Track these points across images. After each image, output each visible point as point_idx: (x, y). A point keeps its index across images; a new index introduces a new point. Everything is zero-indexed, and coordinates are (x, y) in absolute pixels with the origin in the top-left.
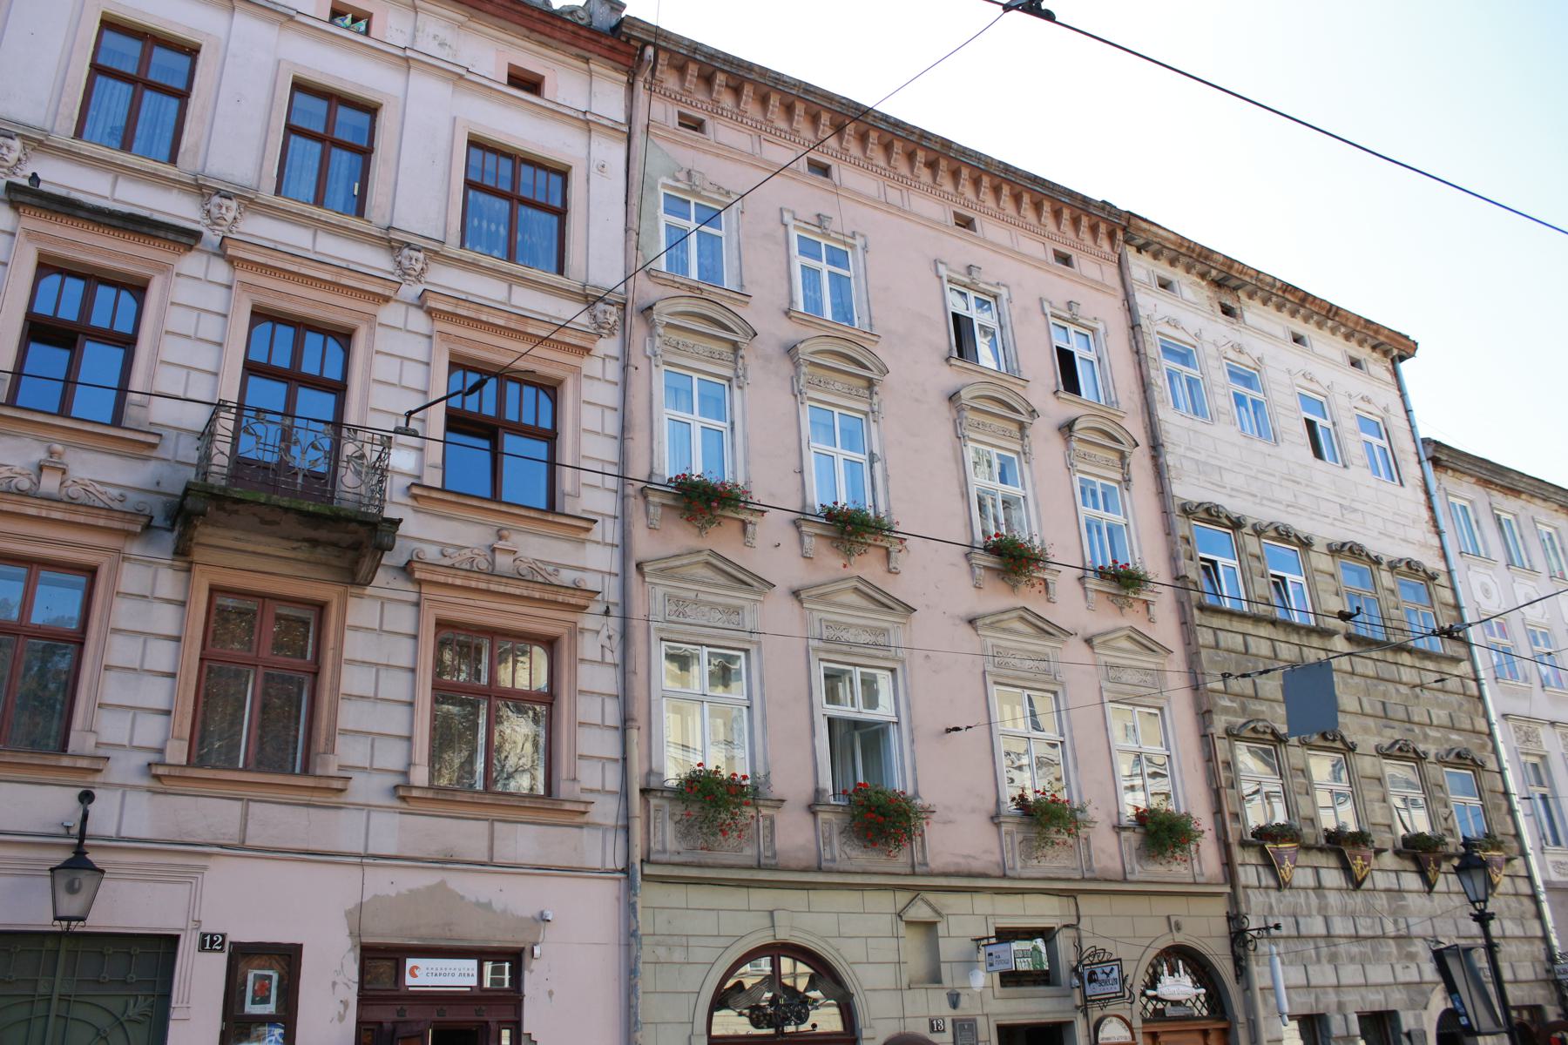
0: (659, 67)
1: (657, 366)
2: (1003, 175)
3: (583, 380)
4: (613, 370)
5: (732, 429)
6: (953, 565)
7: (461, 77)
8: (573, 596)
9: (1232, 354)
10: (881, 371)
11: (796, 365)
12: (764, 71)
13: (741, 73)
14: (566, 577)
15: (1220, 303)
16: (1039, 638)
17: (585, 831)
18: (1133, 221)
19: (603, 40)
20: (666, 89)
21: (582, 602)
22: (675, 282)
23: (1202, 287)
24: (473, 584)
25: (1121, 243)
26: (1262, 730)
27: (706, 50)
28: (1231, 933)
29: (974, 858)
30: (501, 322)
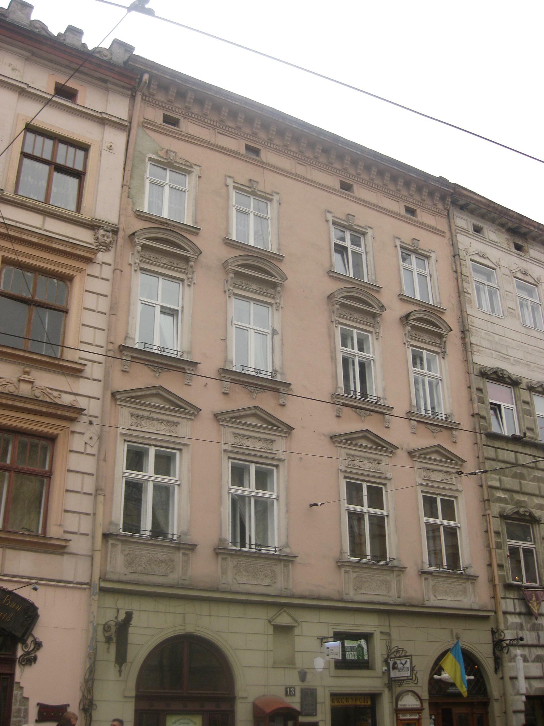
0: (152, 86)
1: (136, 271)
3: (86, 277)
4: (107, 272)
5: (182, 311)
8: (68, 411)
9: (519, 275)
10: (282, 278)
11: (227, 273)
14: (67, 400)
15: (514, 243)
16: (376, 450)
20: (156, 100)
21: (73, 415)
22: (152, 219)
23: (502, 233)
25: (450, 203)
26: (523, 513)
28: (493, 641)
30: (35, 240)
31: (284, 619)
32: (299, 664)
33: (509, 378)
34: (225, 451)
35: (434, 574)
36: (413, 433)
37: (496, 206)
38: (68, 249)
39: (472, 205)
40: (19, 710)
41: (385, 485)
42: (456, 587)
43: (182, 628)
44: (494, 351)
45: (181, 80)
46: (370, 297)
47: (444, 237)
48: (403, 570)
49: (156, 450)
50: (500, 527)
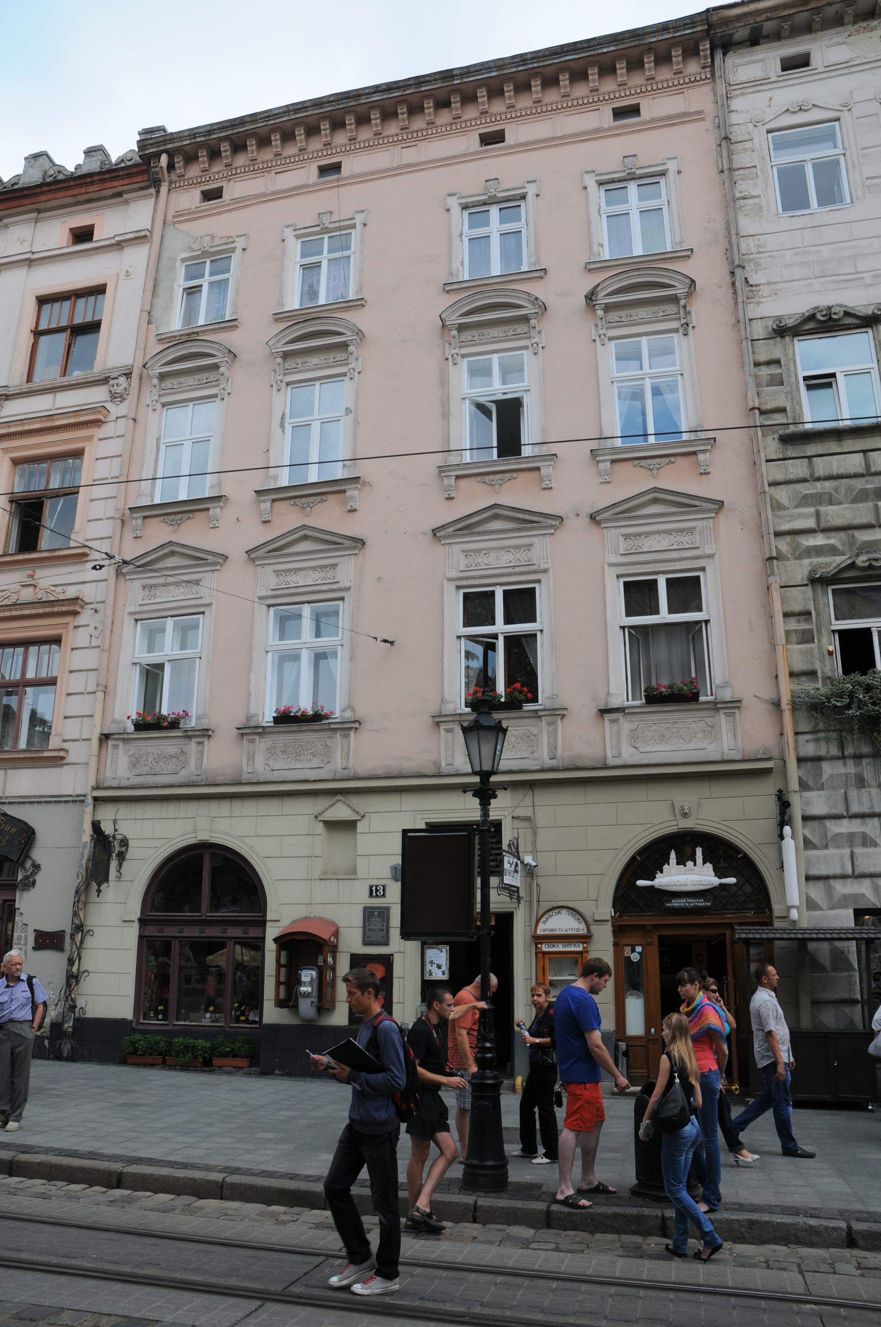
10: (353, 331)
12: (254, 118)
13: (235, 131)
14: (71, 592)
16: (519, 530)
21: (70, 608)
22: (175, 336)
31: (340, 811)
33: (847, 314)
34: (261, 598)
35: (626, 711)
36: (602, 483)
38: (72, 421)
40: (20, 937)
42: (689, 726)
43: (194, 835)
46: (512, 294)
50: (812, 603)
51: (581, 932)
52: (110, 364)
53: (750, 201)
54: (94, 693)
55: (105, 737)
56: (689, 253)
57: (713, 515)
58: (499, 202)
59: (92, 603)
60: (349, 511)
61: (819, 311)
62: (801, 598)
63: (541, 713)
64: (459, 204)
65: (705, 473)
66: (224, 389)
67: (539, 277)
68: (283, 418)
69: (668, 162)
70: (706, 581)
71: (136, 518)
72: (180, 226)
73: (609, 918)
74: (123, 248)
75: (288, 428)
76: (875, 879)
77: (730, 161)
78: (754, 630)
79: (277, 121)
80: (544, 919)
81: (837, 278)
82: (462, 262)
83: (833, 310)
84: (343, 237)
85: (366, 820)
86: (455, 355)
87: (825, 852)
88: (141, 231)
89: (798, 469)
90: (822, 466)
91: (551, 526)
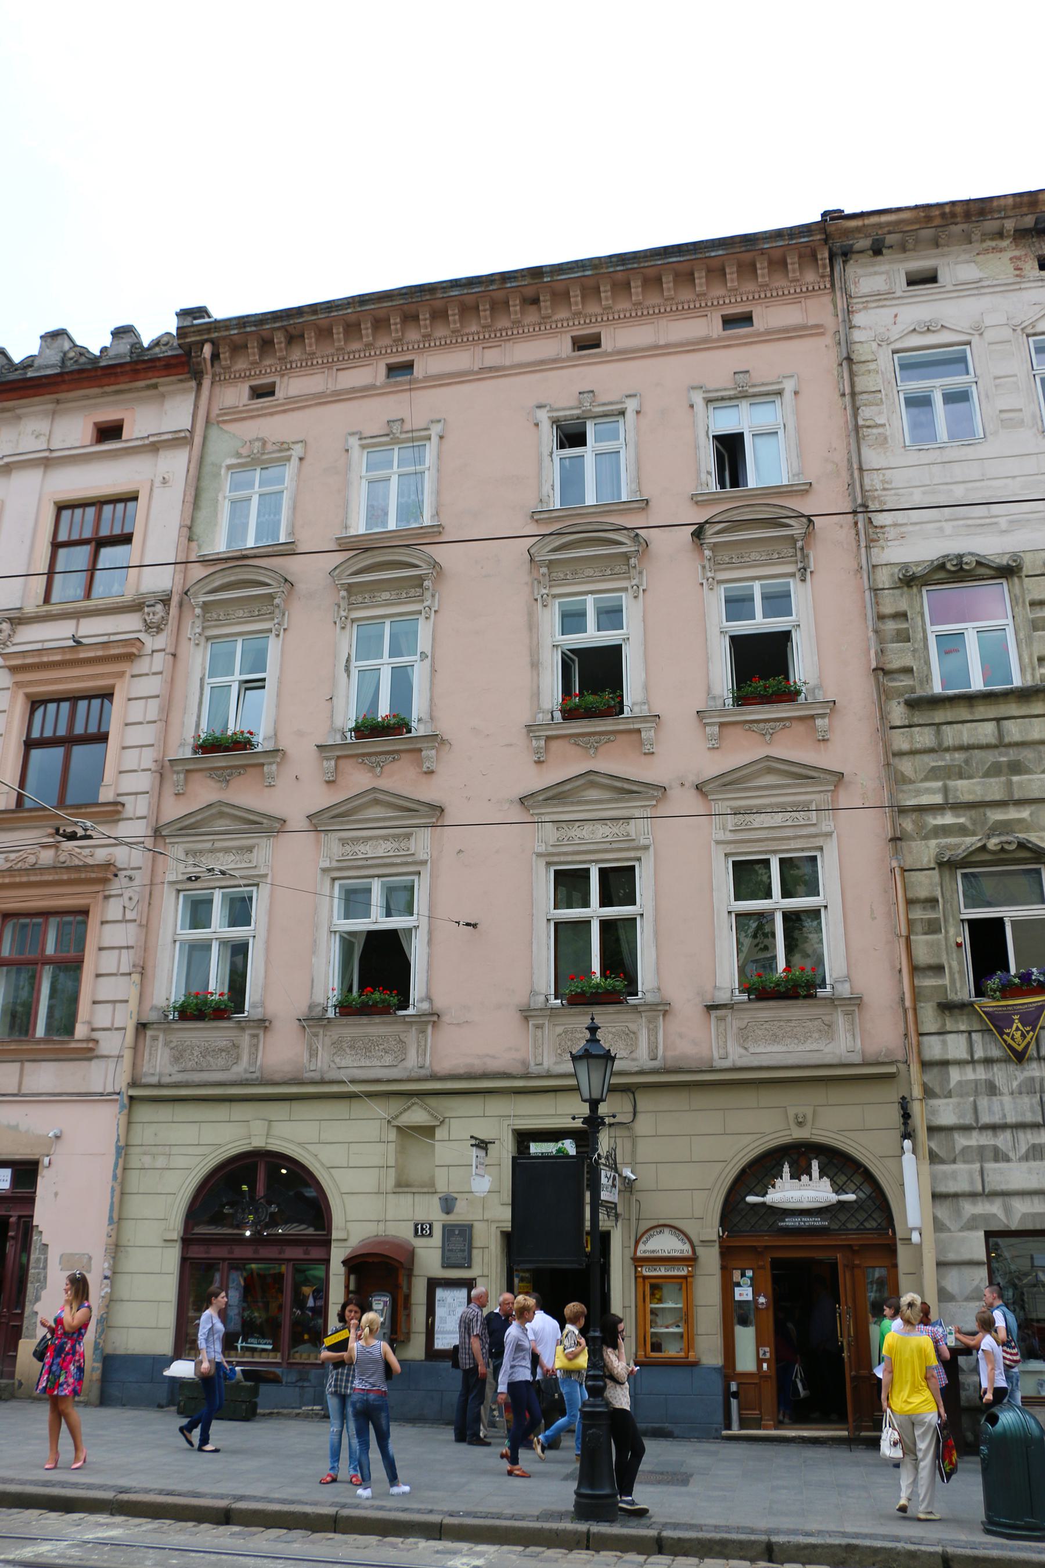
2: (619, 268)
4: (159, 662)
6: (511, 745)
7: (46, 458)
10: (429, 564)
12: (314, 309)
13: (292, 322)
16: (616, 800)
17: (94, 1063)
18: (831, 229)
19: (158, 364)
20: (235, 372)
24: (18, 880)
27: (253, 319)
29: (494, 1057)
30: (57, 658)
31: (417, 1116)
32: (441, 1186)
33: (979, 564)
35: (735, 1007)
36: (709, 749)
37: (947, 209)
38: (100, 653)
39: (888, 237)
41: (639, 859)
43: (247, 1141)
44: (946, 520)
45: (255, 326)
47: (822, 334)
48: (660, 1008)
49: (224, 895)
50: (939, 889)
51: (685, 1254)
52: (144, 589)
53: (875, 431)
54: (130, 974)
55: (142, 1027)
56: (807, 487)
57: (832, 788)
58: (595, 417)
59: (125, 869)
60: (426, 773)
61: (949, 560)
62: (926, 884)
63: (641, 1009)
64: (549, 417)
65: (823, 740)
66: (279, 624)
67: (639, 508)
68: (348, 660)
69: (785, 381)
70: (823, 861)
71: (178, 773)
72: (226, 427)
73: (715, 1237)
74: (157, 450)
75: (354, 673)
76: (1007, 1199)
77: (852, 385)
78: (875, 918)
79: (341, 313)
80: (644, 1239)
81: (970, 522)
82: (553, 486)
83: (965, 560)
84: (416, 449)
85: (445, 1127)
86: (545, 596)
87: (954, 1167)
88: (180, 431)
89: (924, 738)
90: (951, 735)
91: (653, 797)
